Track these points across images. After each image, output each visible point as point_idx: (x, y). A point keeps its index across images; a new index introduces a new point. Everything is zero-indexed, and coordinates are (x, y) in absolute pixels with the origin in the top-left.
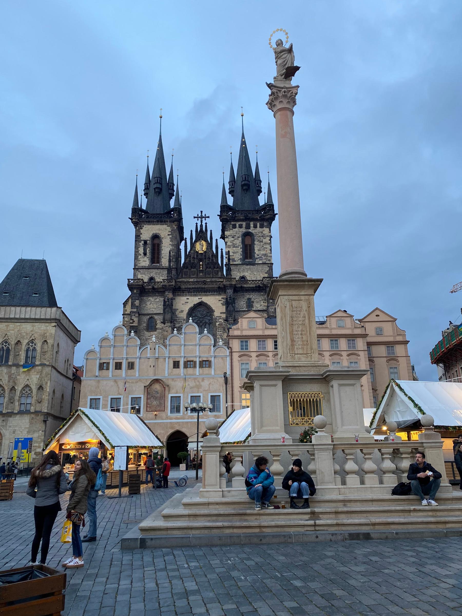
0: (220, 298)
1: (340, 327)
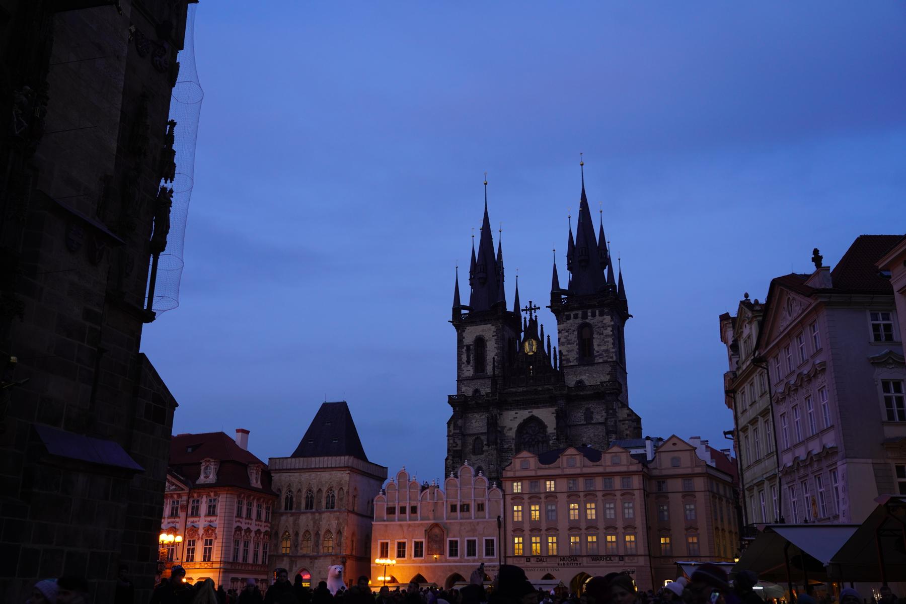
0: (553, 410)
1: (614, 464)
